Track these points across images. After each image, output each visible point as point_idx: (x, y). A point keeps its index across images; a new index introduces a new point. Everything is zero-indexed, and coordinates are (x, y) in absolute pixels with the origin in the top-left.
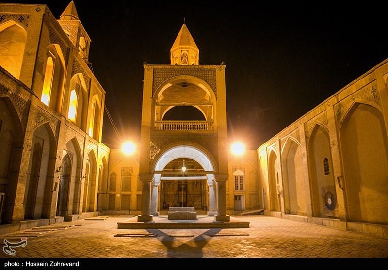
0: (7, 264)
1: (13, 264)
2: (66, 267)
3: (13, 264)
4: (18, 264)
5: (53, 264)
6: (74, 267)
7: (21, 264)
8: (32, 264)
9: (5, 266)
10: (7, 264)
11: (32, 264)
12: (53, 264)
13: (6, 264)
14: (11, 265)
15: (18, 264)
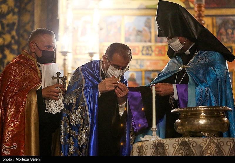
0: (4, 160)
1: (8, 160)
2: (22, 161)
3: (8, 160)
4: (11, 160)
5: (32, 159)
6: (38, 161)
7: (13, 160)
8: (20, 160)
9: (3, 160)
10: (4, 160)
11: (20, 160)
12: (32, 159)
13: (4, 160)
14: (7, 160)
15: (11, 160)
